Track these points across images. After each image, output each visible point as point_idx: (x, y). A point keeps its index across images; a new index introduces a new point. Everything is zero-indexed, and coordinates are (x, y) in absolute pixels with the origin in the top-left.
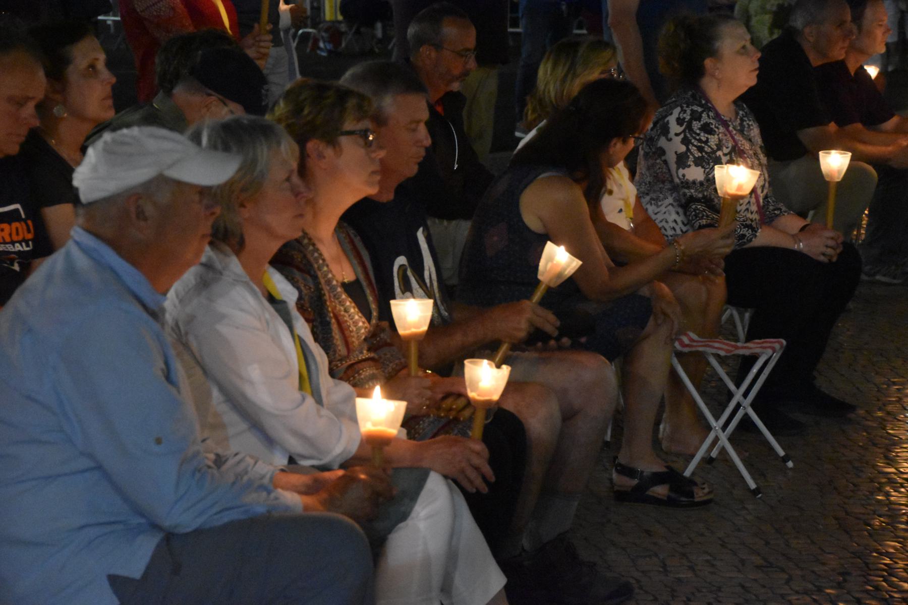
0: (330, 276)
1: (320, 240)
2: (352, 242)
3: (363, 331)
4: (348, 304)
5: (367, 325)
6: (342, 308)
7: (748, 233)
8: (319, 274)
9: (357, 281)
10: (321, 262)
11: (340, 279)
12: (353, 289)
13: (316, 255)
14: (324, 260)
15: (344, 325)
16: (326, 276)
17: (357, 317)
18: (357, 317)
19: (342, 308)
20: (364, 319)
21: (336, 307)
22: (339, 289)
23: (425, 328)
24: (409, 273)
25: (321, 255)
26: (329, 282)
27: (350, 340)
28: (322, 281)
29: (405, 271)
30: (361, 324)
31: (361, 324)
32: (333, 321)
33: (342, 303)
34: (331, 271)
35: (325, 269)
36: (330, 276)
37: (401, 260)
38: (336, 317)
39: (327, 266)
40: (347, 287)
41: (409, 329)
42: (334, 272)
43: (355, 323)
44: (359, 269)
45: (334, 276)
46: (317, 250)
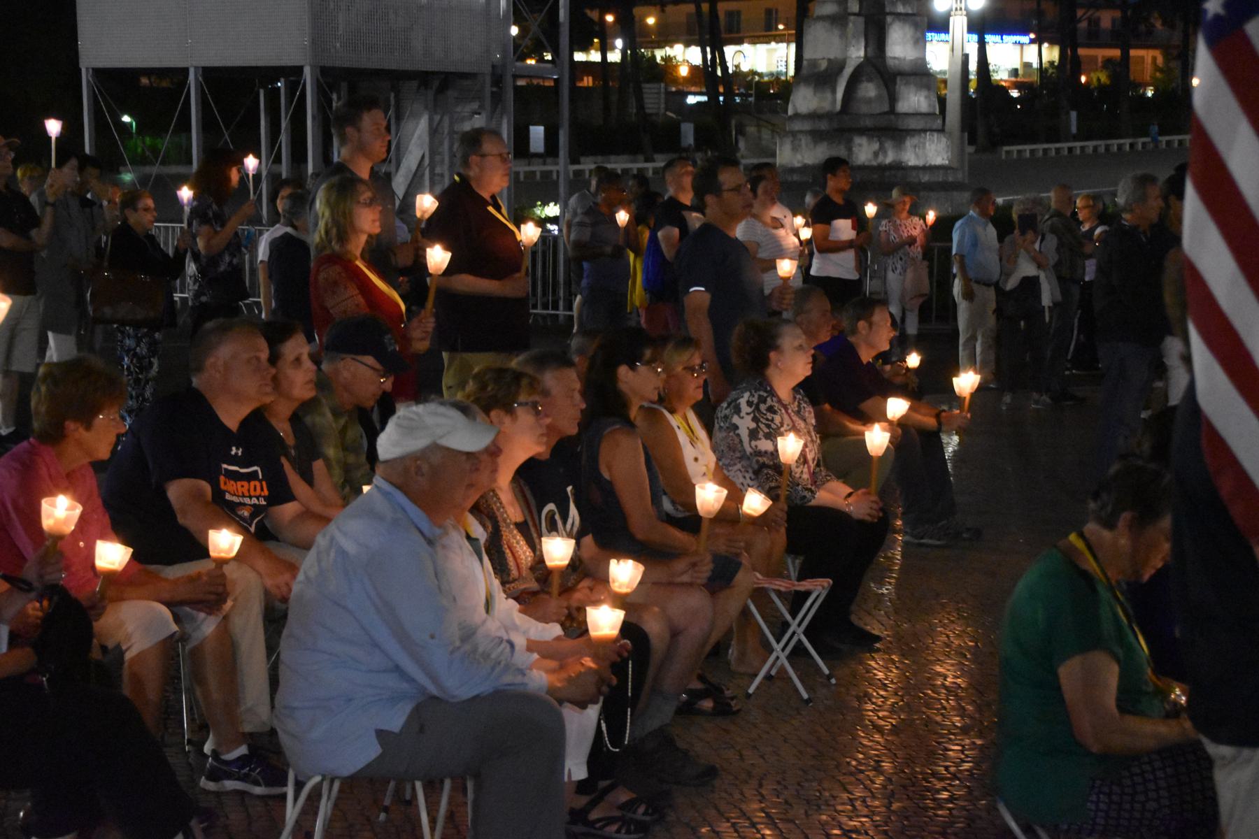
0: (505, 515)
1: (500, 489)
2: (522, 492)
3: (529, 559)
4: (518, 537)
5: (532, 554)
6: (515, 541)
7: (808, 494)
8: (498, 514)
9: (525, 522)
10: (498, 505)
11: (513, 520)
12: (522, 528)
13: (495, 499)
14: (501, 503)
15: (516, 555)
16: (502, 515)
17: (525, 548)
18: (525, 548)
19: (515, 541)
20: (529, 550)
21: (509, 540)
22: (512, 526)
23: (566, 562)
24: (557, 517)
25: (499, 499)
26: (505, 520)
27: (520, 566)
28: (499, 518)
29: (554, 515)
30: (528, 554)
31: (528, 554)
32: (508, 551)
33: (514, 537)
34: (506, 512)
35: (502, 510)
36: (505, 515)
37: (551, 506)
38: (510, 548)
39: (503, 508)
40: (517, 525)
41: (554, 561)
42: (509, 512)
43: (524, 553)
44: (526, 512)
45: (508, 516)
46: (496, 495)
